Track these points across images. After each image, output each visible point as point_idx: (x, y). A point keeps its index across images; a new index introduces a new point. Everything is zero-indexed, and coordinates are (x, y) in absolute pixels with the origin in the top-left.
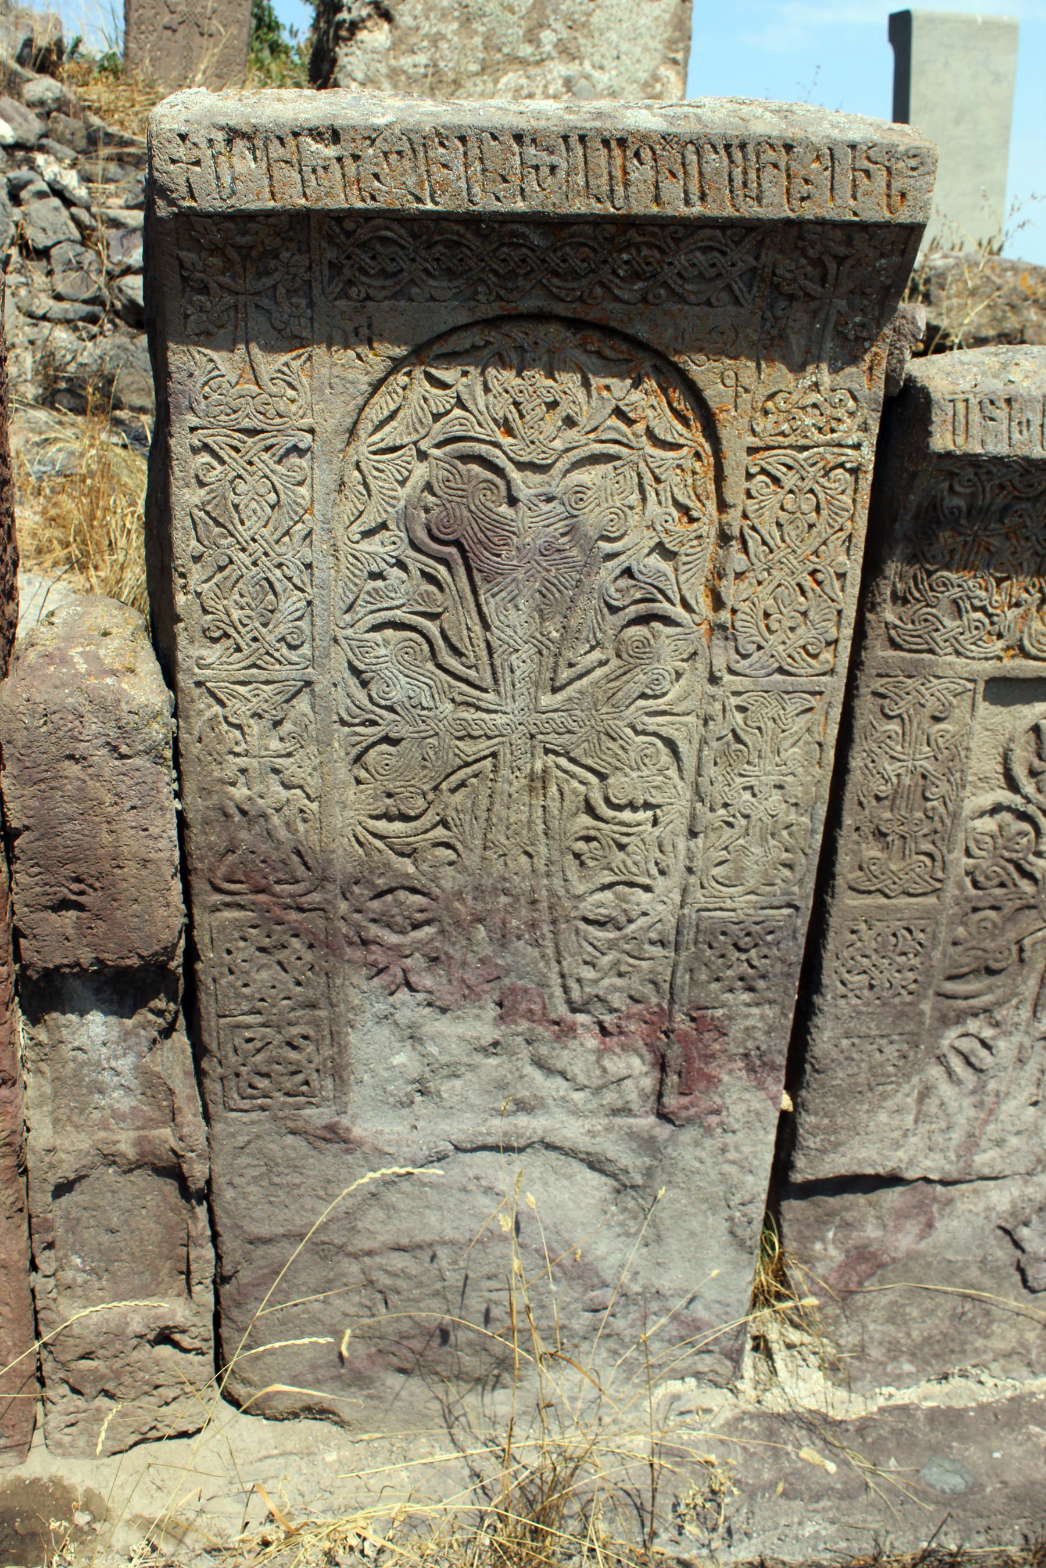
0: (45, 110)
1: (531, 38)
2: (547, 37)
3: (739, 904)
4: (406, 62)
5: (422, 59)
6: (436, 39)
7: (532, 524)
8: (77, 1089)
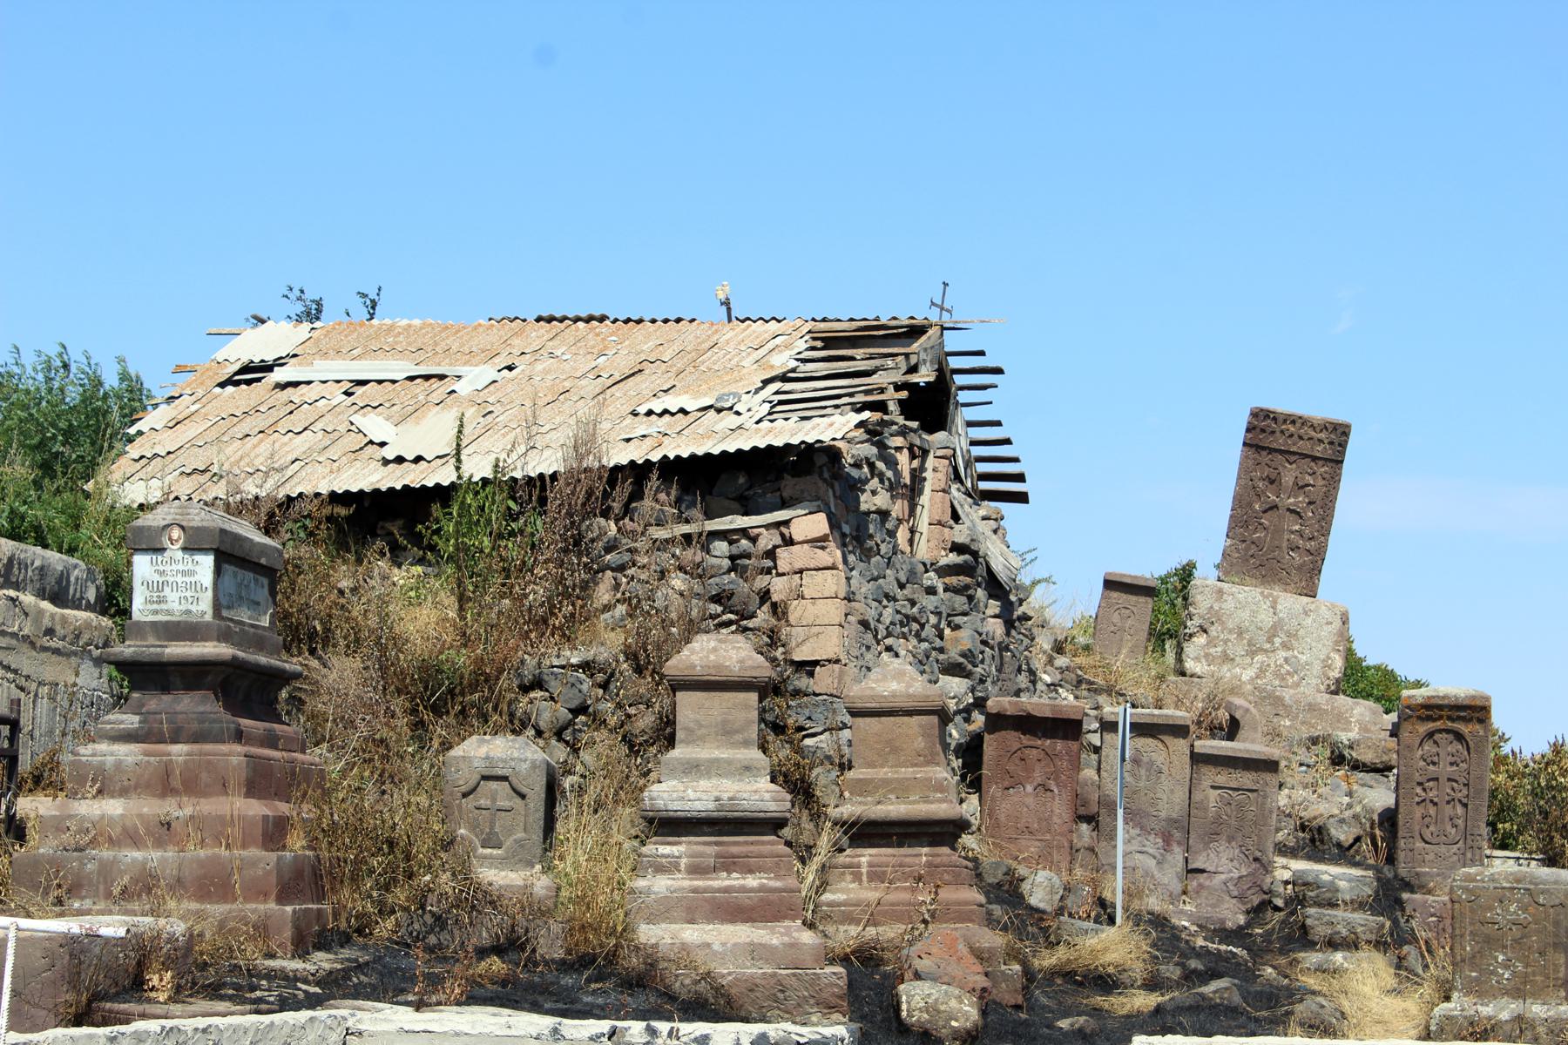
0: (1062, 670)
1: (1270, 640)
2: (1277, 641)
3: (1174, 815)
4: (1212, 650)
5: (1219, 649)
6: (1226, 642)
7: (1145, 759)
8: (1080, 837)
